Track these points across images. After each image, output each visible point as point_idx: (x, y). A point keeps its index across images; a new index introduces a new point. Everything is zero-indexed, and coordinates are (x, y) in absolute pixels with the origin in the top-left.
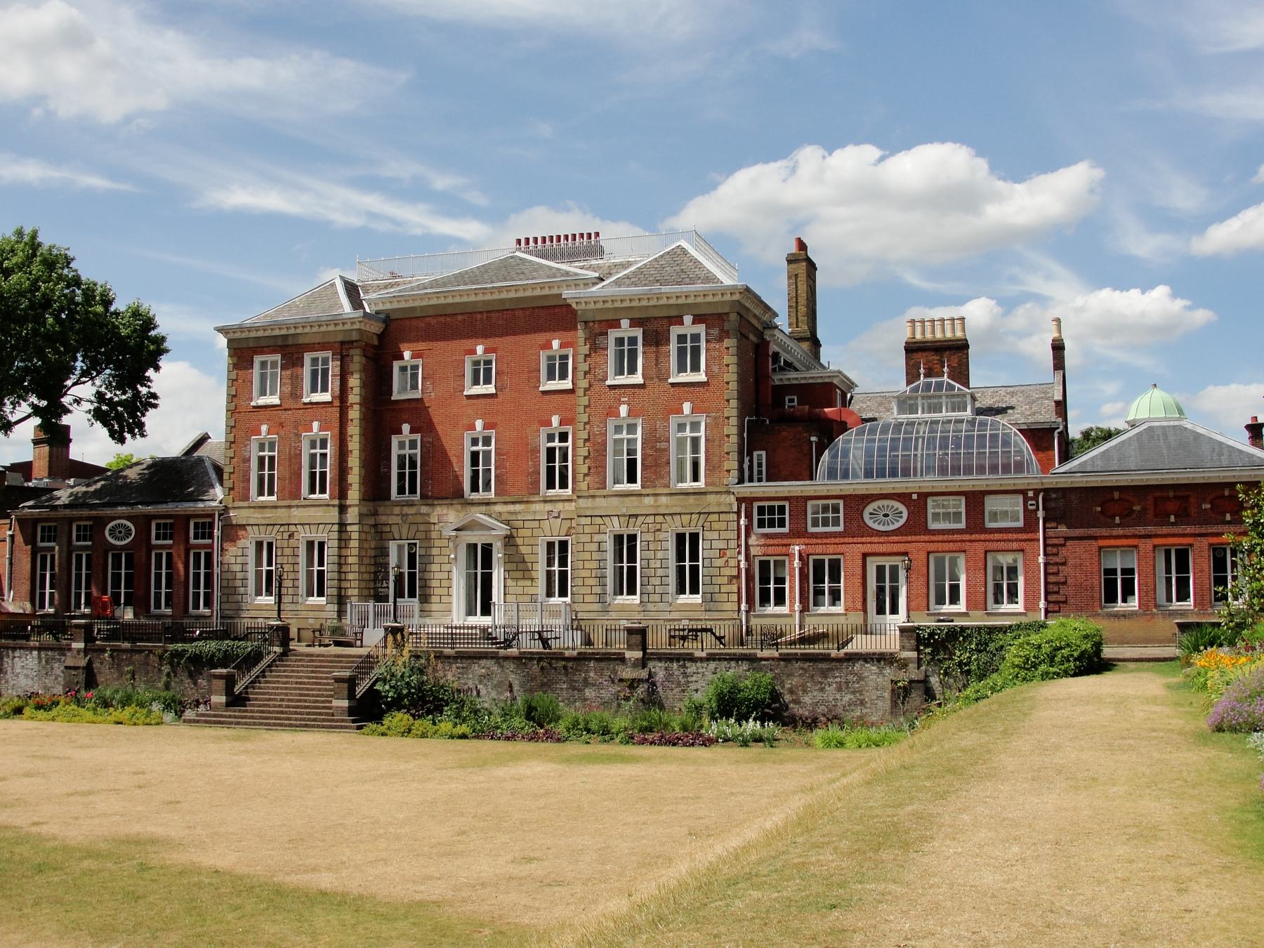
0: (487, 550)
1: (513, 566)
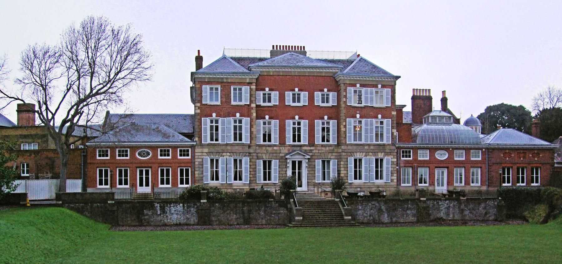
0: (300, 163)
1: (310, 169)
